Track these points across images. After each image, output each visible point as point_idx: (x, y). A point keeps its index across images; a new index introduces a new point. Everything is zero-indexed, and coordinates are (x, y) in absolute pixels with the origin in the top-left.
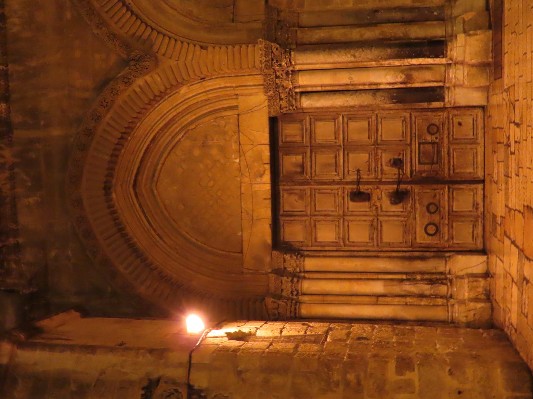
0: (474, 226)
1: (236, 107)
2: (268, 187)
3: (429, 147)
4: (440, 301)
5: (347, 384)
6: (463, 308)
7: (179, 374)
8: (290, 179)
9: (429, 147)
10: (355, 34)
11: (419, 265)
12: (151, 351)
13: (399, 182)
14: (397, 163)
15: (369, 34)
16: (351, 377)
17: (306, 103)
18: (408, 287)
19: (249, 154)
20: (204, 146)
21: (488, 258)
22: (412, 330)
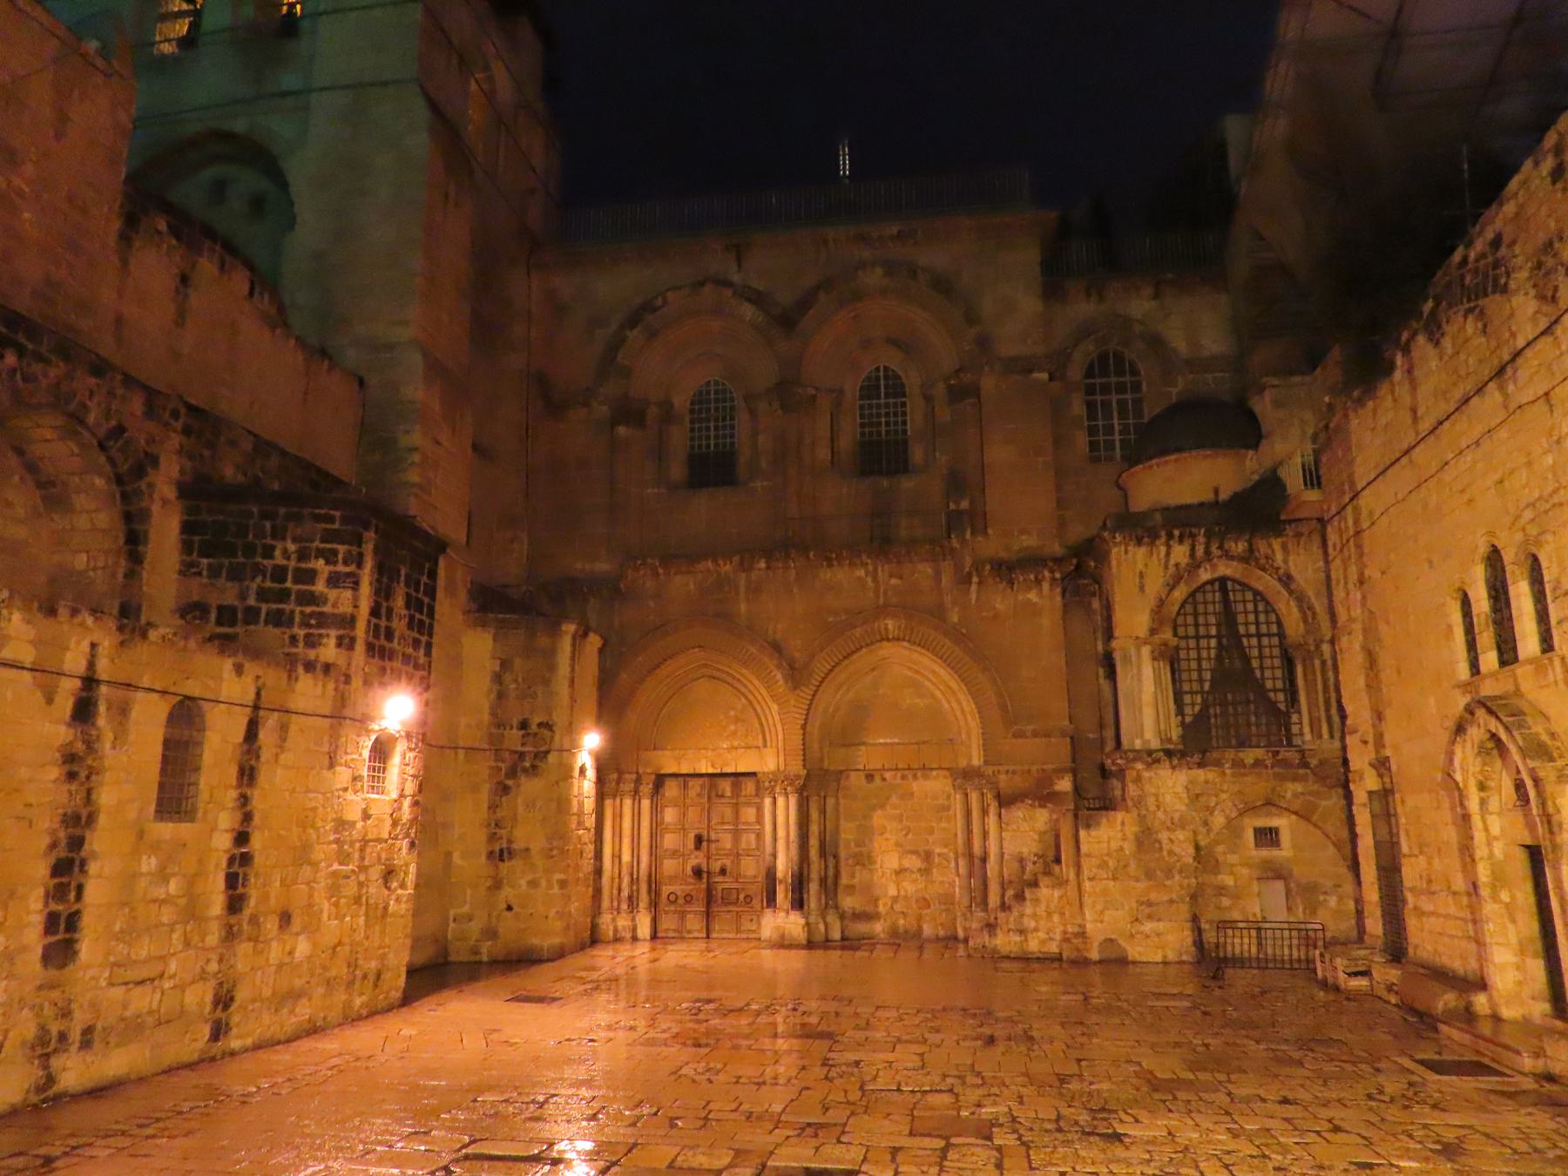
0: (674, 931)
1: (765, 746)
2: (704, 771)
3: (735, 896)
4: (615, 904)
5: (551, 850)
6: (609, 921)
7: (556, 744)
8: (713, 787)
9: (734, 897)
10: (814, 842)
11: (644, 888)
12: (571, 724)
13: (708, 872)
14: (723, 872)
15: (814, 853)
16: (555, 852)
17: (768, 801)
18: (626, 880)
19: (729, 756)
20: (737, 720)
21: (645, 940)
22: (588, 886)
